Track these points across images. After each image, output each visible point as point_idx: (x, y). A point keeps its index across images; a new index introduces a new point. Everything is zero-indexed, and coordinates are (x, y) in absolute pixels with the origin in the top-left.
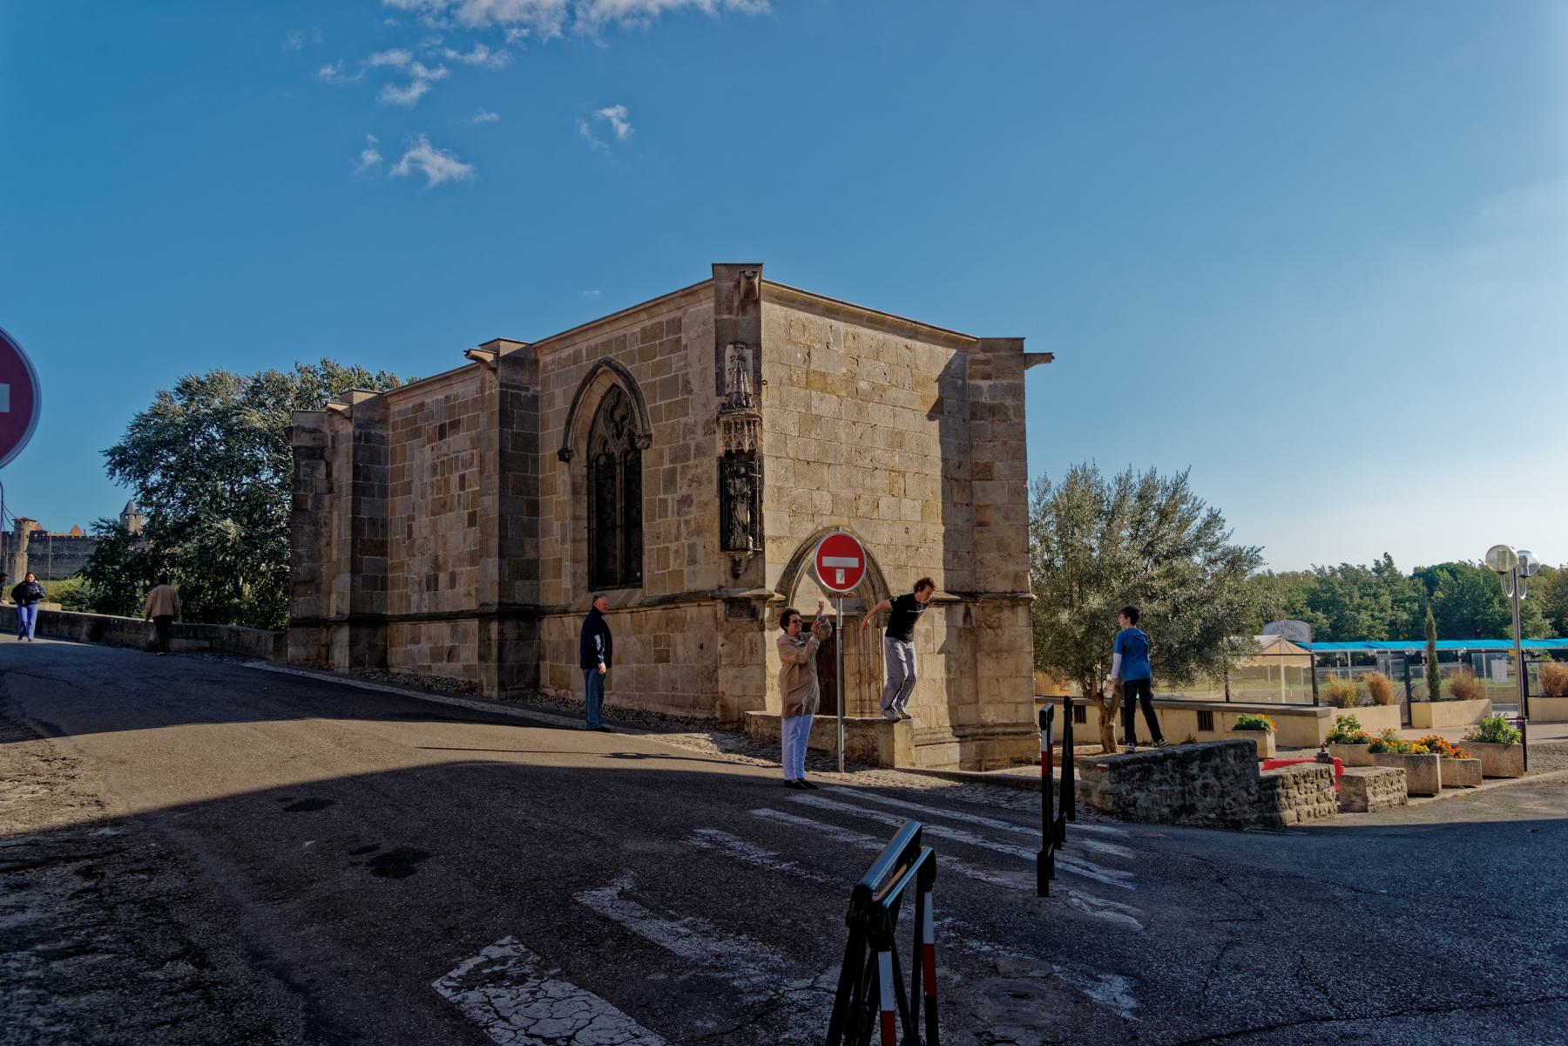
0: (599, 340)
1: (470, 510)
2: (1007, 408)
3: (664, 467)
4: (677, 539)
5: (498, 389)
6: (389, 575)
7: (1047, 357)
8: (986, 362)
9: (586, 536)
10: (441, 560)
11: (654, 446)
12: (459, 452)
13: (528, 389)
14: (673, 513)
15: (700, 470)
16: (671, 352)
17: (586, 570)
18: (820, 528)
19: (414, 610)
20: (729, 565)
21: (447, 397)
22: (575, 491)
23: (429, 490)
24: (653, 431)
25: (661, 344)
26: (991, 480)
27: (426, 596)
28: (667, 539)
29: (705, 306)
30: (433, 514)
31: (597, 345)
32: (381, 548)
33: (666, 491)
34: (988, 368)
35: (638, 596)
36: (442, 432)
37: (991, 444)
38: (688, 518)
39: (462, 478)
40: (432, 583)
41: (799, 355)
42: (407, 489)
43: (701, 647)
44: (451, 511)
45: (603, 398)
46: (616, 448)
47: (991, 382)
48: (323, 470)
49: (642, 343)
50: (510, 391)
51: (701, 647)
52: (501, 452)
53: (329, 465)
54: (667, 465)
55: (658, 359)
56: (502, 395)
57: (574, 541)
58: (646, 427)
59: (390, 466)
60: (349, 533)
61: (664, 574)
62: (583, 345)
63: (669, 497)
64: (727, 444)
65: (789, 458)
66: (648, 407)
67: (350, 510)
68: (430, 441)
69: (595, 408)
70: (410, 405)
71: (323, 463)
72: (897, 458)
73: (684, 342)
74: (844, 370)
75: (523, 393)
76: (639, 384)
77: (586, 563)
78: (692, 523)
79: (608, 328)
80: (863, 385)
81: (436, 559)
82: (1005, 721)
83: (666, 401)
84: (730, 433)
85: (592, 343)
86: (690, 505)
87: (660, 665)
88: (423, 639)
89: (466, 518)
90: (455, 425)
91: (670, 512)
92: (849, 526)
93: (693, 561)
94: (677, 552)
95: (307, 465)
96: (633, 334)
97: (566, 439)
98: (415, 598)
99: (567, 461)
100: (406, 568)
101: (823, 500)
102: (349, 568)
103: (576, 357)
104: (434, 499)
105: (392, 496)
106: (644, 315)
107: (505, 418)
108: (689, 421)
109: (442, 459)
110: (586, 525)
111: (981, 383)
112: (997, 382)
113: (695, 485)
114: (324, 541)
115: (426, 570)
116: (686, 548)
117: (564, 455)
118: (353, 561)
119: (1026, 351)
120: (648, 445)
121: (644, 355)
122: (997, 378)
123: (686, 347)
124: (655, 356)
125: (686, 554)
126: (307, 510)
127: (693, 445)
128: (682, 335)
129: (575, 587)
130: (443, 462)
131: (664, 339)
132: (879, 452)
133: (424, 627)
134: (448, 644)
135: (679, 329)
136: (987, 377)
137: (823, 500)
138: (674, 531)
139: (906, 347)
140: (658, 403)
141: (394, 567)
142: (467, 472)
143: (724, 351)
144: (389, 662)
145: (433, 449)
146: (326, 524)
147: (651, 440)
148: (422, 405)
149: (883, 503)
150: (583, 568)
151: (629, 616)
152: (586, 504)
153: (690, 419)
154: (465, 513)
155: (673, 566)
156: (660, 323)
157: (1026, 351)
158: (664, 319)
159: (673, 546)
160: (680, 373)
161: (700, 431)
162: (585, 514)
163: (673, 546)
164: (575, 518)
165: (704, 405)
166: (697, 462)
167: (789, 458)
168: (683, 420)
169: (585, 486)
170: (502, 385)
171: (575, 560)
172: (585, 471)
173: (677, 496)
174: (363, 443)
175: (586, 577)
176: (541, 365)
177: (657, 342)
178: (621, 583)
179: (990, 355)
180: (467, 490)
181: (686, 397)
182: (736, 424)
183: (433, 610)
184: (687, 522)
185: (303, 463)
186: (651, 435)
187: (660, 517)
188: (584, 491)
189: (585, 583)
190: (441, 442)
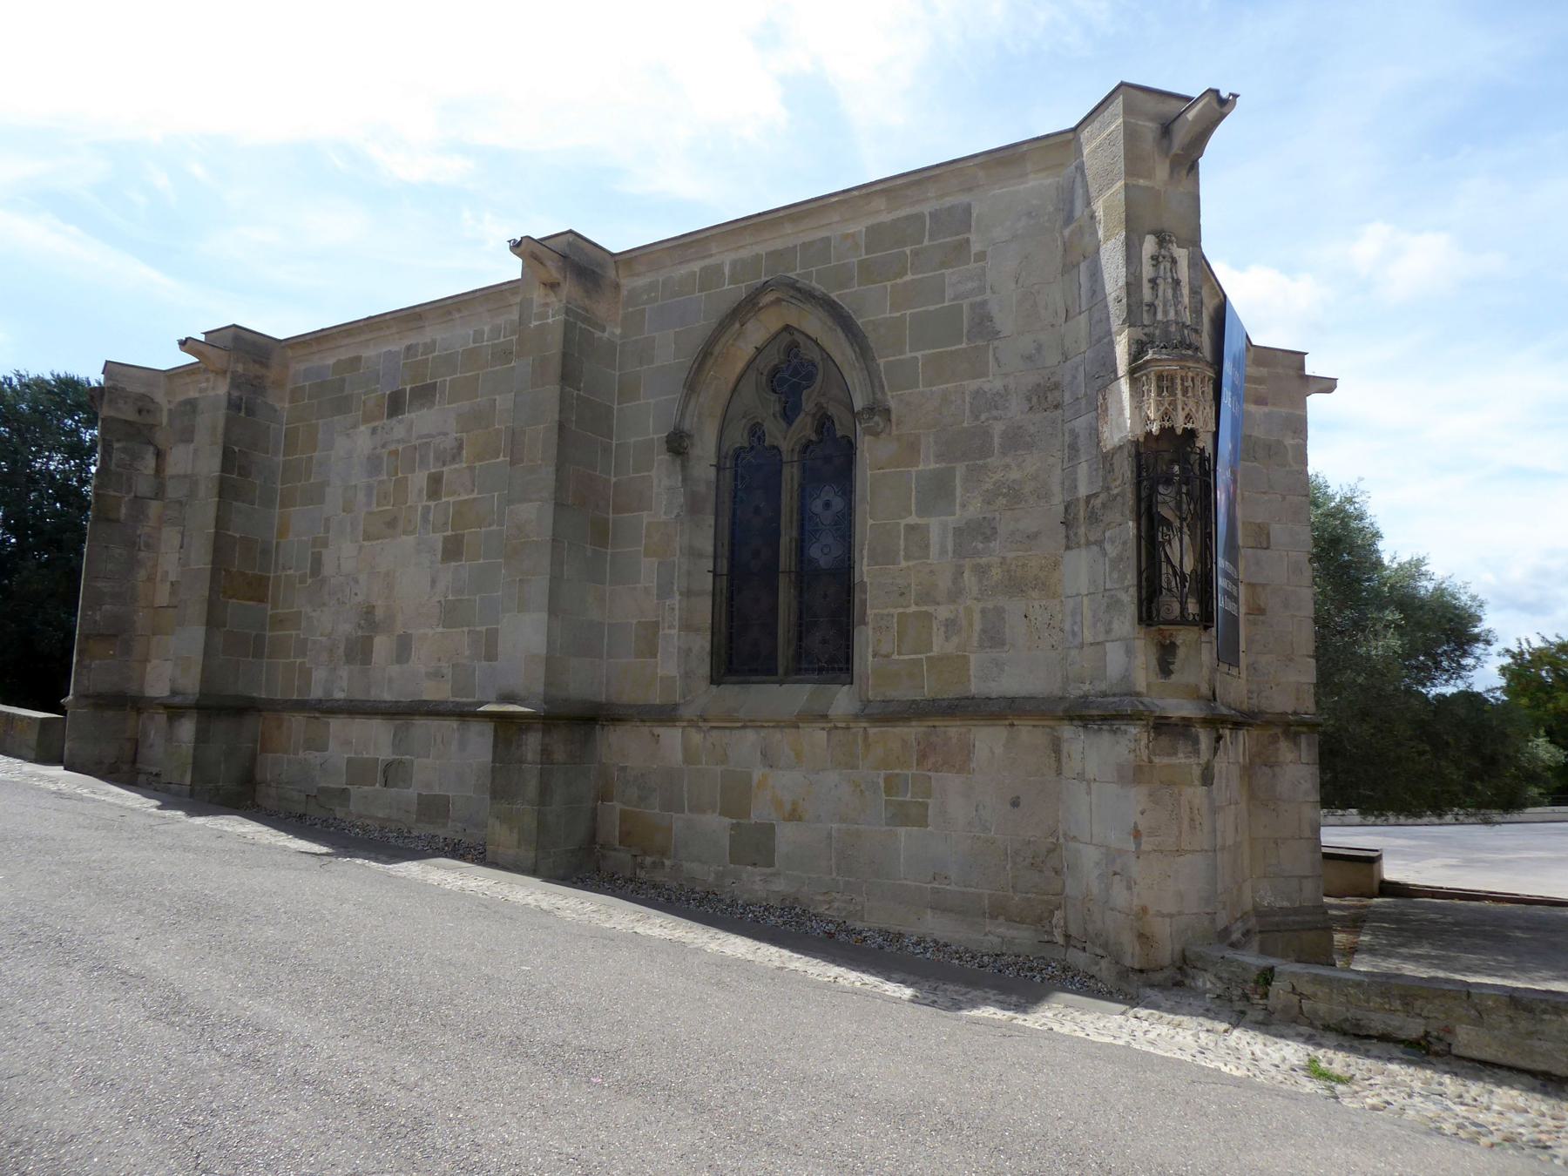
0: (761, 249)
1: (449, 533)
2: (1285, 447)
3: (921, 467)
4: (955, 595)
5: (561, 317)
6: (268, 634)
9: (710, 587)
10: (379, 614)
12: (432, 436)
13: (603, 330)
14: (943, 551)
15: (1015, 475)
16: (943, 265)
17: (708, 646)
19: (316, 693)
21: (409, 348)
22: (693, 507)
23: (361, 497)
24: (892, 404)
25: (916, 254)
26: (1267, 548)
27: (344, 672)
28: (926, 597)
29: (1031, 184)
30: (368, 537)
31: (758, 257)
32: (258, 588)
33: (923, 511)
34: (1262, 388)
35: (842, 700)
36: (395, 405)
38: (984, 561)
39: (435, 482)
40: (359, 651)
42: (316, 495)
43: (1015, 803)
44: (405, 533)
45: (759, 350)
46: (786, 439)
47: (1266, 409)
48: (150, 461)
49: (866, 254)
50: (579, 324)
51: (1015, 803)
52: (562, 427)
53: (159, 455)
54: (928, 464)
55: (909, 277)
56: (568, 327)
57: (688, 594)
58: (879, 395)
59: (281, 458)
60: (209, 558)
61: (918, 662)
62: (725, 258)
63: (934, 524)
64: (1166, 416)
66: (881, 362)
67: (213, 523)
68: (366, 420)
69: (739, 366)
70: (331, 361)
71: (151, 449)
73: (976, 248)
75: (598, 334)
76: (859, 322)
77: (709, 633)
79: (788, 228)
81: (370, 611)
82: (1286, 904)
83: (927, 352)
85: (744, 253)
86: (987, 539)
87: (902, 831)
88: (332, 744)
89: (440, 546)
90: (425, 394)
91: (934, 550)
93: (993, 637)
95: (124, 450)
96: (846, 237)
98: (319, 675)
100: (304, 624)
102: (204, 620)
103: (710, 276)
104: (370, 513)
105: (283, 505)
106: (880, 203)
107: (568, 376)
108: (986, 387)
109: (393, 447)
111: (1252, 408)
113: (1002, 501)
114: (142, 574)
115: (346, 628)
116: (977, 617)
117: (678, 444)
118: (212, 605)
119: (1308, 371)
121: (868, 272)
122: (1274, 404)
123: (981, 256)
124: (903, 273)
125: (977, 627)
126: (118, 521)
127: (998, 428)
128: (973, 237)
129: (687, 675)
130: (395, 453)
131: (926, 242)
133: (336, 724)
134: (385, 754)
135: (968, 227)
136: (1260, 401)
138: (944, 583)
140: (909, 355)
141: (279, 622)
142: (445, 469)
143: (1141, 245)
144: (258, 777)
145: (374, 431)
146: (148, 546)
148: (358, 359)
150: (702, 643)
151: (824, 734)
152: (712, 531)
153: (992, 383)
154: (437, 539)
155: (939, 646)
156: (919, 217)
157: (1308, 371)
158: (926, 209)
159: (943, 612)
160: (965, 304)
161: (1016, 408)
162: (710, 549)
163: (943, 612)
164: (694, 553)
165: (1030, 358)
166: (1008, 460)
168: (972, 385)
169: (713, 498)
170: (568, 311)
171: (687, 627)
172: (712, 472)
173: (956, 518)
174: (242, 414)
175: (708, 660)
176: (624, 292)
177: (908, 250)
178: (786, 673)
179: (1264, 371)
180: (444, 500)
181: (980, 343)
183: (359, 695)
184: (981, 571)
185: (116, 445)
187: (907, 558)
188: (710, 506)
189: (705, 669)
190: (394, 421)
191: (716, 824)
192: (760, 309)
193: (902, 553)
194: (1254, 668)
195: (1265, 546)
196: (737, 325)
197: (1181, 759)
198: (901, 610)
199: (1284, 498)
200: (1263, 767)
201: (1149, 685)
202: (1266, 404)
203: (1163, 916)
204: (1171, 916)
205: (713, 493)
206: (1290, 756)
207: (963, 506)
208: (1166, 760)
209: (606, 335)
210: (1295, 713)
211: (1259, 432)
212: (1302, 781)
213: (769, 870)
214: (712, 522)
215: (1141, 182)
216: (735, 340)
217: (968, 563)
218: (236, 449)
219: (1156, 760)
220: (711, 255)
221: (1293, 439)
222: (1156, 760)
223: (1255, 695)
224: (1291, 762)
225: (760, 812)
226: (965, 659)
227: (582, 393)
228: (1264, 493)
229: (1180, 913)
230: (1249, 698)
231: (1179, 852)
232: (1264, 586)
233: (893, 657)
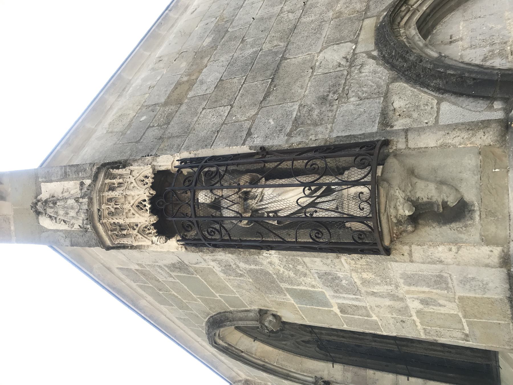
11: (274, 309)
18: (375, 53)
24: (256, 307)
41: (143, 119)
58: (252, 314)
78: (365, 275)
92: (378, 16)
94: (425, 302)
110: (406, 378)
125: (427, 289)
132: (285, 8)
147: (267, 311)
159: (414, 305)
163: (414, 305)
186: (260, 311)
192: (229, 344)
193: (366, 318)
196: (243, 354)
198: (418, 324)
201: (486, 241)
205: (351, 368)
207: (313, 286)
216: (252, 354)
217: (363, 289)
226: (461, 299)
233: (468, 332)
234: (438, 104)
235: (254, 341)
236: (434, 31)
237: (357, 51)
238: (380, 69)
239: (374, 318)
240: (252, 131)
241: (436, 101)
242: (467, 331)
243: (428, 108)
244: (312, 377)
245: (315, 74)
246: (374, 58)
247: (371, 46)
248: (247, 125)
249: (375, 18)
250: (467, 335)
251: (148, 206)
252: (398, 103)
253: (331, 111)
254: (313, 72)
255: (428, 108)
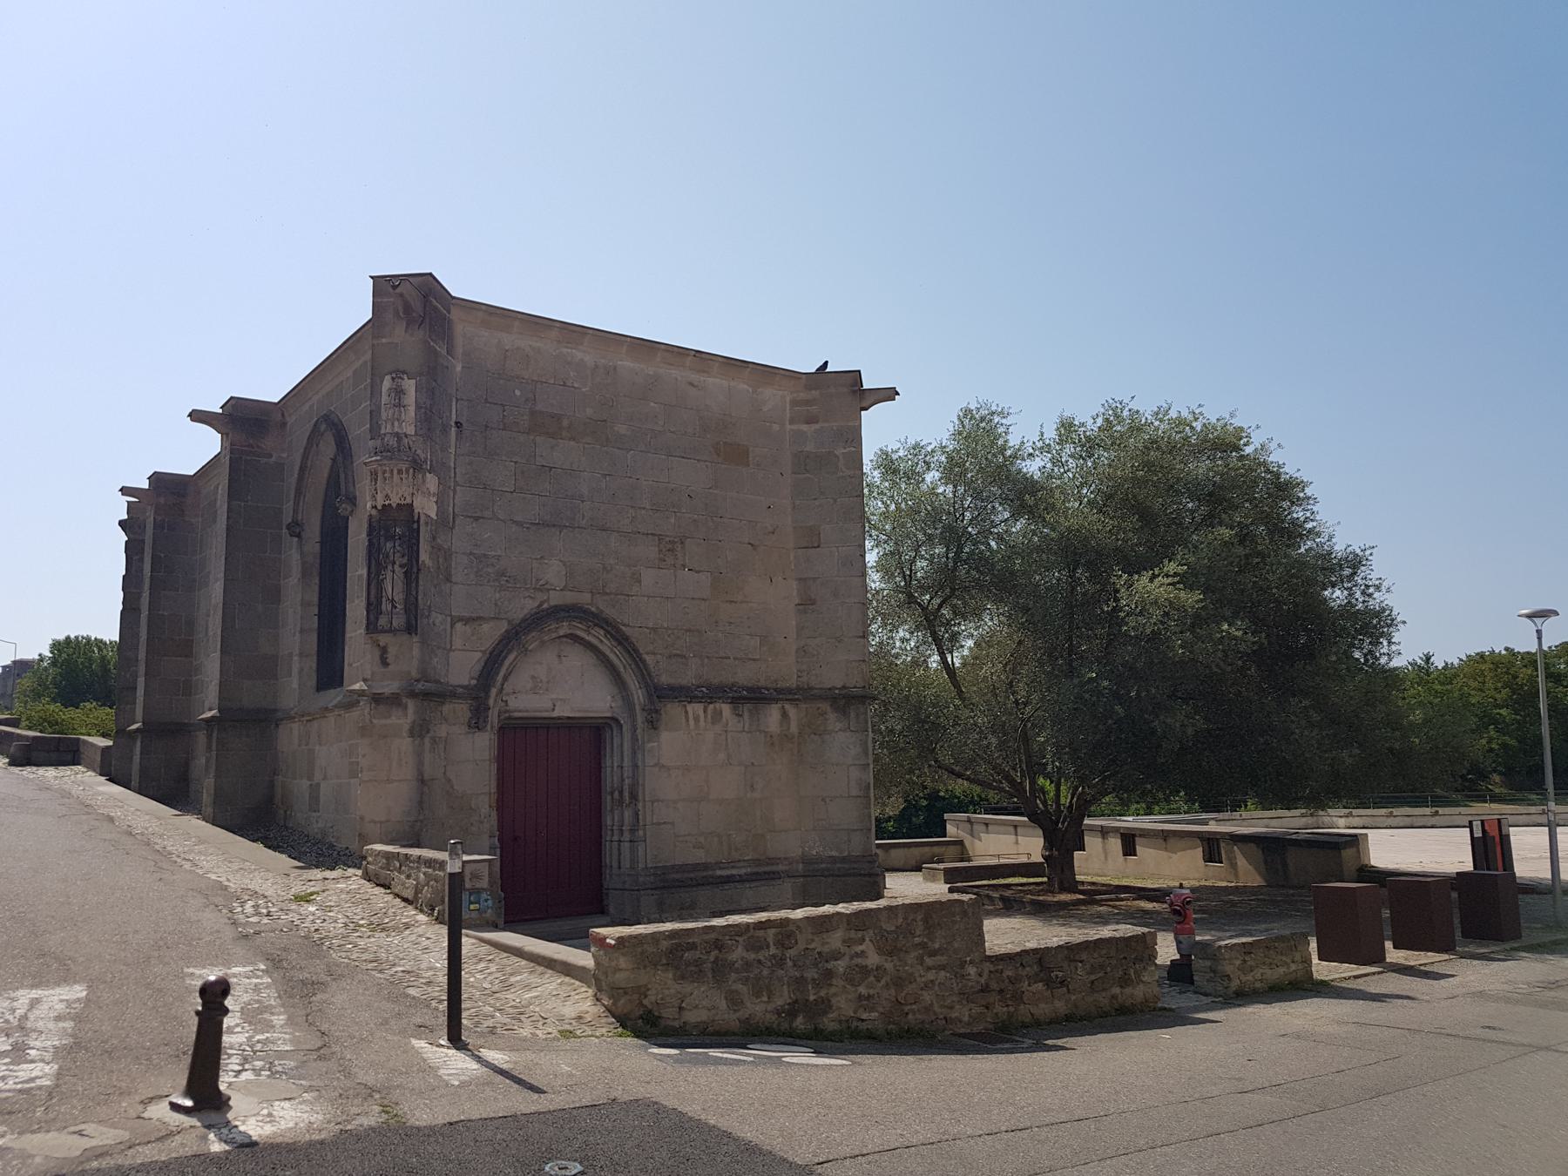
7: (890, 394)
8: (807, 402)
9: (316, 625)
13: (271, 456)
17: (314, 666)
18: (545, 606)
20: (377, 653)
22: (305, 573)
26: (818, 547)
37: (817, 503)
41: (518, 393)
47: (817, 426)
58: (351, 489)
64: (374, 497)
65: (498, 519)
72: (673, 520)
74: (589, 411)
75: (264, 460)
77: (315, 657)
80: (622, 429)
84: (376, 483)
97: (295, 511)
99: (299, 536)
101: (553, 573)
110: (316, 612)
111: (804, 427)
112: (826, 425)
120: (352, 511)
136: (811, 420)
137: (553, 573)
139: (692, 384)
149: (649, 577)
150: (312, 663)
162: (315, 600)
167: (498, 519)
179: (815, 393)
182: (384, 472)
189: (313, 682)
191: (305, 783)
194: (804, 651)
195: (816, 545)
197: (393, 720)
199: (835, 501)
200: (813, 736)
201: (373, 674)
202: (817, 422)
203: (375, 822)
204: (381, 822)
205: (318, 561)
206: (839, 725)
208: (383, 722)
209: (273, 459)
210: (844, 687)
211: (810, 447)
212: (851, 747)
213: (318, 814)
214: (317, 581)
215: (384, 340)
218: (162, 555)
219: (375, 721)
220: (310, 399)
221: (845, 448)
222: (375, 721)
223: (805, 674)
224: (840, 730)
225: (318, 776)
227: (250, 503)
228: (815, 499)
229: (388, 821)
230: (799, 677)
231: (389, 781)
232: (815, 579)
234: (481, 651)
235: (331, 459)
236: (577, 644)
237: (551, 592)
238: (526, 611)
239: (356, 602)
240: (481, 520)
241: (483, 649)
242: (354, 665)
243: (478, 645)
244: (302, 519)
245: (534, 561)
246: (540, 605)
247: (553, 603)
248: (487, 514)
249: (590, 602)
250: (351, 665)
251: (387, 503)
252: (486, 627)
253: (489, 581)
254: (537, 559)
255: (478, 645)
